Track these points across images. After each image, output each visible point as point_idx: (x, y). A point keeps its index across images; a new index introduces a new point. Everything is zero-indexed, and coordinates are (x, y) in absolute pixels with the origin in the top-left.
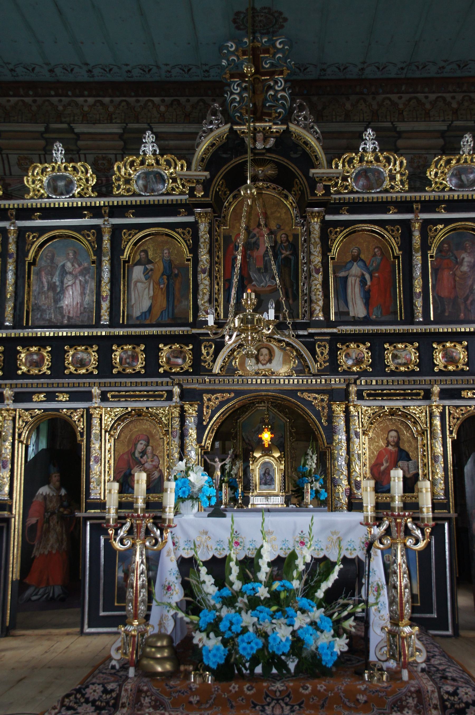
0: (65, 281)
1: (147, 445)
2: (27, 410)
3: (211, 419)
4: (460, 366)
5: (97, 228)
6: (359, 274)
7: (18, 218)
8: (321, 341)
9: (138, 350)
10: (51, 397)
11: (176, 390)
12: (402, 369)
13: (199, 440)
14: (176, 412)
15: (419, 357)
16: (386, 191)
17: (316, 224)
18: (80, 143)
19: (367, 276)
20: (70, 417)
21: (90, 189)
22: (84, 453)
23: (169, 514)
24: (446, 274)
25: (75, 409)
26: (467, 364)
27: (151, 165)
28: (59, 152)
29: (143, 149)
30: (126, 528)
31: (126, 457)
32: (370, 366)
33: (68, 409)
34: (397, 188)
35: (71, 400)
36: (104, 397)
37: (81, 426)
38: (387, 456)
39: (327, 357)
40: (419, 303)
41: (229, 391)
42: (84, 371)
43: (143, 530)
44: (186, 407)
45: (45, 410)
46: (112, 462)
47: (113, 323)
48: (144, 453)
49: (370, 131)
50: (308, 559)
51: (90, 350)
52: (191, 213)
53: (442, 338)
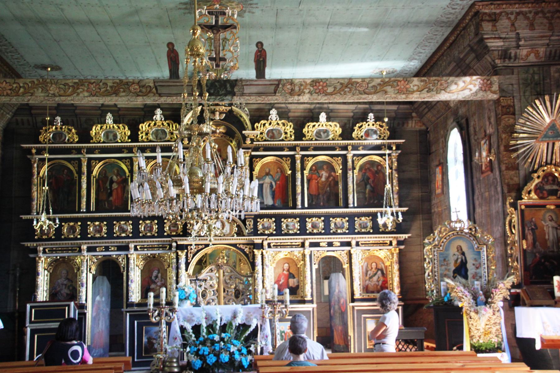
0: (113, 186)
2: (94, 256)
3: (192, 259)
4: (320, 230)
5: (131, 158)
6: (269, 182)
7: (87, 153)
8: (249, 218)
9: (153, 223)
10: (107, 249)
11: (174, 244)
12: (291, 232)
13: (187, 270)
14: (174, 255)
15: (299, 226)
16: (283, 140)
18: (120, 112)
19: (274, 184)
20: (117, 259)
21: (127, 137)
22: (125, 278)
23: (176, 306)
24: (314, 182)
25: (120, 255)
26: (323, 229)
28: (109, 119)
29: (154, 118)
30: (157, 312)
31: (147, 279)
32: (275, 230)
33: (116, 255)
34: (289, 139)
35: (118, 250)
36: (136, 249)
37: (123, 263)
38: (283, 277)
39: (252, 226)
40: (299, 198)
41: (202, 245)
42: (123, 235)
43: (164, 313)
44: (180, 253)
45: (104, 256)
46: (140, 282)
48: (156, 277)
49: (274, 109)
50: (237, 325)
51: (128, 224)
53: (311, 216)
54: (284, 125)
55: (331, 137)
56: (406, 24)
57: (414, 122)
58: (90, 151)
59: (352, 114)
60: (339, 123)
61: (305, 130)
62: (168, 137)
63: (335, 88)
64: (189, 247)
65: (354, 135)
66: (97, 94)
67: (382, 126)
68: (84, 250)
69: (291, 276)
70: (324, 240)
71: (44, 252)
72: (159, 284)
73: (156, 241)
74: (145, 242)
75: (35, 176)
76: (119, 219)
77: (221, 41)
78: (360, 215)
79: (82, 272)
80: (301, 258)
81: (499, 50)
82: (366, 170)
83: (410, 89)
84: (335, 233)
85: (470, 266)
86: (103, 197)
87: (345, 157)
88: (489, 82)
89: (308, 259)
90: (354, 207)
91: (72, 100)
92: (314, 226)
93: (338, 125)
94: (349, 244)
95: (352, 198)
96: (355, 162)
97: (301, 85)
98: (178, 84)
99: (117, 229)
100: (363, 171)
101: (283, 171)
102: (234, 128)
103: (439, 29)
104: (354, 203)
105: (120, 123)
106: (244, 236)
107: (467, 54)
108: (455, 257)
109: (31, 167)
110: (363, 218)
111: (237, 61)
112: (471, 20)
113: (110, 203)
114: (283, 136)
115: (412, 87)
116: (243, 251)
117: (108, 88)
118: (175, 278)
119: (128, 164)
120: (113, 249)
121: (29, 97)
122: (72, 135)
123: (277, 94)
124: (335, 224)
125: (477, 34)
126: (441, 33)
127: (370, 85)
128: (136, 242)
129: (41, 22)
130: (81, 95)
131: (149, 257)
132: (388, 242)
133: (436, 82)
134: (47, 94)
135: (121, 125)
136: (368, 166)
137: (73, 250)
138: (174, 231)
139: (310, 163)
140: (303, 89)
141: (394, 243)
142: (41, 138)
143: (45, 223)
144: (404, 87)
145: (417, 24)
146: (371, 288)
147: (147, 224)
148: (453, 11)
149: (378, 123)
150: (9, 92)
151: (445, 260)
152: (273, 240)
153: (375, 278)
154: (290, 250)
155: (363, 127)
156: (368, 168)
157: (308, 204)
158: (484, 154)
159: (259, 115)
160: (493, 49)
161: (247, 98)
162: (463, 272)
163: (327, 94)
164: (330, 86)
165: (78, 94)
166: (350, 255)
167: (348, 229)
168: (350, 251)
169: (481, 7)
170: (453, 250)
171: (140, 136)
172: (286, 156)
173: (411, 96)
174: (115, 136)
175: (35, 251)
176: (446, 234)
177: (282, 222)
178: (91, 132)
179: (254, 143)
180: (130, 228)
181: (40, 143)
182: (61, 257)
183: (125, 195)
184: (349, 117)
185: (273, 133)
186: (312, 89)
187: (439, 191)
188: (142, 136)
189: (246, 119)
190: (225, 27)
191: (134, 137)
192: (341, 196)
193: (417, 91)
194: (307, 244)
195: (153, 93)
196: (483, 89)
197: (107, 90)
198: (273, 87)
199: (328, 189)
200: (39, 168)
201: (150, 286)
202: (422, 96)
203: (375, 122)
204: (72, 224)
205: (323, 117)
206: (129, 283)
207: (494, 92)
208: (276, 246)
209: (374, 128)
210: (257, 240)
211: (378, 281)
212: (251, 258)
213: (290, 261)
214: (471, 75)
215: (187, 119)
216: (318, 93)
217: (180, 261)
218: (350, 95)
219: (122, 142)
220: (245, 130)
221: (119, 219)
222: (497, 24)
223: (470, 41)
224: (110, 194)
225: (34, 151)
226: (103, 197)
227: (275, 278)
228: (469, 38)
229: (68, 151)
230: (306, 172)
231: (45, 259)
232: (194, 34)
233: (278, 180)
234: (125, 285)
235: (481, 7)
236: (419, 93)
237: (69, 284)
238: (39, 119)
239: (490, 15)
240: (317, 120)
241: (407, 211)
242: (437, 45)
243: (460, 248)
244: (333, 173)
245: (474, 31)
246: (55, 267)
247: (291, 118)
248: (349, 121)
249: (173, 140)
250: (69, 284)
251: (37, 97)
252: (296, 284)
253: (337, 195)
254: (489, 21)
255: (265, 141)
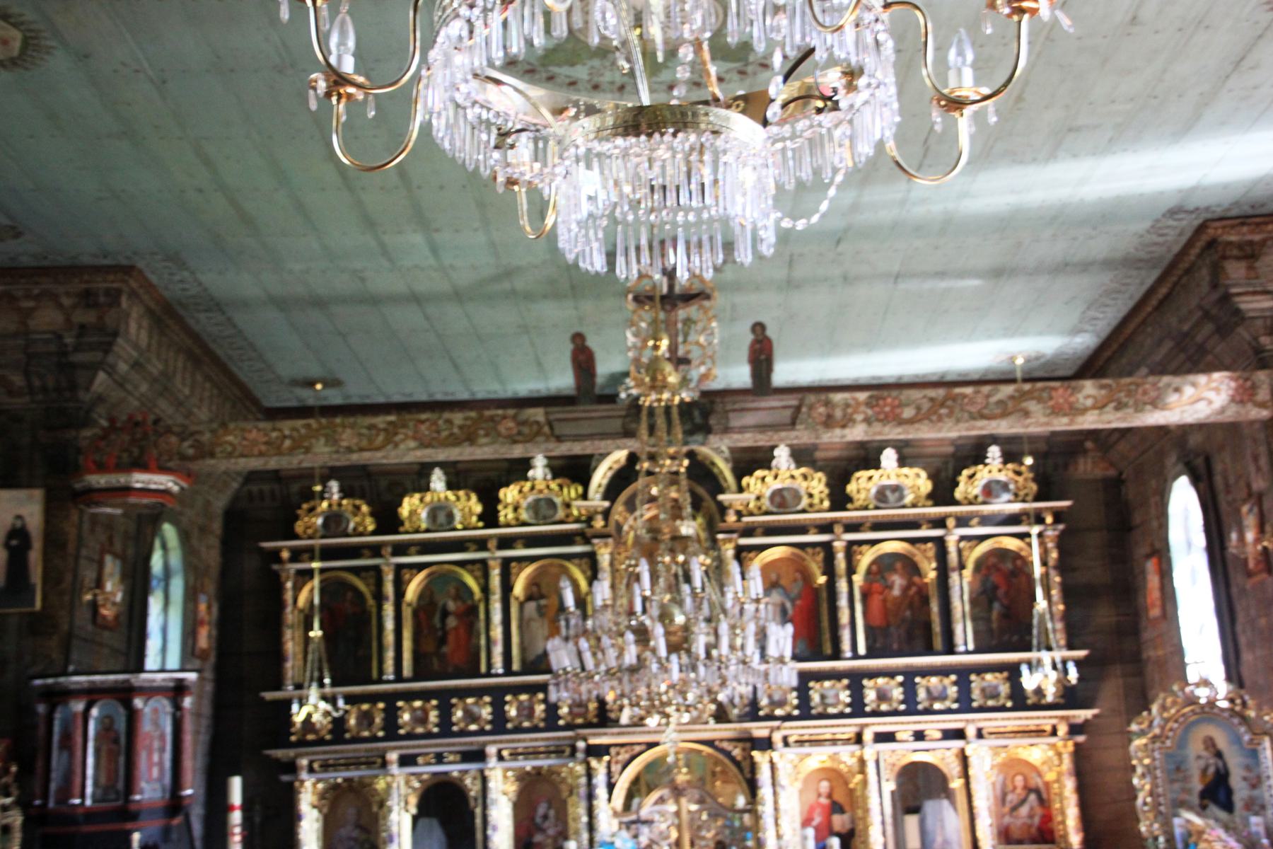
1: (549, 808)
2: (413, 774)
5: (484, 562)
10: (440, 759)
11: (581, 745)
12: (831, 710)
14: (580, 769)
16: (804, 511)
17: (729, 551)
19: (788, 605)
22: (478, 821)
24: (876, 601)
25: (466, 772)
26: (902, 702)
27: (541, 491)
28: (438, 481)
32: (797, 707)
33: (460, 771)
34: (816, 508)
38: (818, 811)
41: (639, 744)
42: (473, 727)
44: (594, 763)
45: (435, 774)
47: (508, 671)
48: (545, 817)
52: (587, 541)
53: (873, 674)
54: (805, 477)
55: (909, 499)
56: (1063, 268)
57: (1089, 460)
58: (400, 549)
59: (950, 449)
60: (924, 468)
61: (851, 488)
62: (561, 514)
63: (919, 408)
64: (613, 751)
65: (958, 494)
66: (434, 443)
67: (1018, 473)
68: (391, 763)
69: (836, 808)
70: (904, 726)
71: (311, 770)
72: (551, 832)
73: (543, 739)
74: (519, 741)
75: (289, 609)
76: (463, 693)
77: (680, 326)
78: (981, 669)
79: (390, 810)
80: (856, 768)
81: (1265, 318)
82: (988, 568)
83: (1077, 406)
84: (928, 711)
85: (1237, 781)
86: (429, 647)
87: (940, 543)
88: (1249, 384)
89: (871, 769)
90: (967, 652)
91: (384, 457)
92: (882, 696)
93: (923, 474)
94: (959, 734)
95: (964, 633)
96: (965, 553)
97: (847, 405)
98: (593, 414)
99: (459, 714)
100: (984, 572)
101: (807, 577)
102: (701, 491)
103: (1134, 273)
104: (966, 644)
105: (459, 488)
106: (729, 721)
107: (1198, 325)
108: (1202, 763)
109: (280, 589)
110: (989, 677)
111: (713, 362)
112: (1200, 256)
113: (442, 657)
114: (805, 502)
115: (1081, 400)
116: (728, 754)
117: (456, 430)
118: (585, 819)
119: (478, 573)
120: (451, 758)
121: (302, 457)
122: (363, 519)
123: (798, 427)
124: (928, 690)
125: (1214, 286)
126: (1137, 281)
127: (993, 399)
128: (501, 742)
129: (319, 303)
130: (402, 446)
131: (528, 773)
132: (1048, 728)
133: (1133, 387)
134: (334, 449)
135: (461, 493)
136: (993, 560)
137: (369, 764)
138: (579, 715)
139: (866, 558)
140: (852, 414)
141: (1063, 730)
142: (299, 527)
143: (316, 707)
144: (1066, 400)
145: (1085, 267)
146: (1016, 834)
147: (521, 703)
148: (1161, 240)
149: (1010, 466)
150: (263, 448)
151: (1178, 769)
152: (795, 730)
153: (1024, 810)
154: (829, 750)
155: (978, 476)
156: (994, 566)
157: (869, 648)
158: (1250, 536)
159: (752, 461)
160: (1251, 314)
161: (736, 436)
162: (1222, 796)
163: (902, 422)
164: (907, 405)
165: (396, 445)
166: (964, 759)
167: (956, 701)
168: (963, 751)
169: (1220, 231)
170: (1195, 748)
171: (502, 513)
172: (813, 545)
173: (1080, 419)
174: (450, 516)
175: (292, 768)
176: (1178, 711)
177: (810, 689)
178: (400, 510)
179: (745, 519)
180: (486, 712)
181: (296, 537)
182: (346, 780)
183: (474, 641)
184: (946, 456)
185: (783, 497)
186: (870, 412)
187: (1155, 612)
188: (506, 514)
189: (724, 469)
190: (689, 297)
191: (489, 517)
192: (937, 627)
193: (1094, 407)
194: (868, 736)
195: (545, 434)
196: (1238, 398)
197: (451, 434)
198: (788, 413)
199: (908, 613)
200: (297, 589)
201: (531, 835)
202: (1106, 417)
203: (1005, 463)
204: (365, 707)
205: (889, 457)
206: (489, 832)
207: (1262, 405)
208: (800, 743)
209: (1002, 477)
210: (759, 730)
211: (1031, 816)
212: (747, 770)
213: (834, 775)
214: (1208, 369)
215: (601, 476)
216: (886, 419)
217: (594, 781)
218: (949, 423)
219: (465, 529)
220: (722, 491)
221: (463, 693)
222: (1257, 264)
223: (1202, 299)
224: (443, 641)
225: (285, 555)
226: (429, 647)
227: (802, 813)
228: (1199, 293)
229: (354, 551)
230: (858, 579)
231: (314, 785)
232: (656, 347)
233: (799, 596)
234: (479, 836)
235: (1220, 231)
236: (1096, 412)
237: (364, 836)
238: (295, 488)
239: (1240, 246)
240: (877, 466)
241: (1086, 657)
242: (1131, 304)
243: (1210, 743)
244: (916, 579)
245: (1207, 278)
246: (332, 801)
247: (820, 463)
248: (946, 463)
249: (571, 519)
250: (364, 836)
251: (316, 454)
252: (848, 826)
253: (928, 626)
254: (1238, 258)
255: (767, 513)
